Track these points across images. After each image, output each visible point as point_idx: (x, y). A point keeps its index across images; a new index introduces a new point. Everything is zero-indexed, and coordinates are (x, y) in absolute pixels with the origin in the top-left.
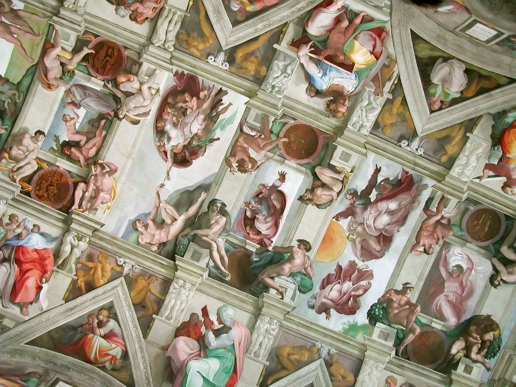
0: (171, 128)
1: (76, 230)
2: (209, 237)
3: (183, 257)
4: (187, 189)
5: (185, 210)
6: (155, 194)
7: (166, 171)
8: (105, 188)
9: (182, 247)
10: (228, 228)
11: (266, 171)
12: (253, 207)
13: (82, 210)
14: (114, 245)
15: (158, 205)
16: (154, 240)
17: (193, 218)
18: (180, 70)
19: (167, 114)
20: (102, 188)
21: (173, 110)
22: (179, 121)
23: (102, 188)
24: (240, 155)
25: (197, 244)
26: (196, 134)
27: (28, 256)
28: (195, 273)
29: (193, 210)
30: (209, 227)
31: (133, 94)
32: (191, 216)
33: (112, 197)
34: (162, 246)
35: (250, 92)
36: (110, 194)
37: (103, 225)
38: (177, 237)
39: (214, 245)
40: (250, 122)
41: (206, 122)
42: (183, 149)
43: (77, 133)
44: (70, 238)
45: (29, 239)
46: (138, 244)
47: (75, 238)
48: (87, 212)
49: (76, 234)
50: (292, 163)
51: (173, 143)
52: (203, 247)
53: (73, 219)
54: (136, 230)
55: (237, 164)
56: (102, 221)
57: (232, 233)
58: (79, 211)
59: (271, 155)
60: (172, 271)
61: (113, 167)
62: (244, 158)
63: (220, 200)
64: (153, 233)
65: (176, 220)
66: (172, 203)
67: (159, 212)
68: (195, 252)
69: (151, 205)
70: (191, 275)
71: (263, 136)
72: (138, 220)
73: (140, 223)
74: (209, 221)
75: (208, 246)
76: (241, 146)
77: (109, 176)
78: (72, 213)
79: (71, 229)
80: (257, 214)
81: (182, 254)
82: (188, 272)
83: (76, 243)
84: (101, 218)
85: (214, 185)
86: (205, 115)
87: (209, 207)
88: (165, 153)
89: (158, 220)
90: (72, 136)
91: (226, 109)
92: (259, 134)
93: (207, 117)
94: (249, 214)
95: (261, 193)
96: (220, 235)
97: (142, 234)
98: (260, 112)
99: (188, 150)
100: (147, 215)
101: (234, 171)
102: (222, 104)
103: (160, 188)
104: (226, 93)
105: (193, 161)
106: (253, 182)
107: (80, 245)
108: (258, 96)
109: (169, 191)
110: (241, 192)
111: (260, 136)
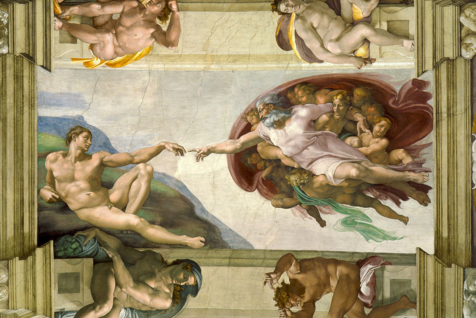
0: (302, 118)
1: (12, 18)
2: (119, 289)
3: (56, 257)
4: (193, 202)
5: (151, 219)
6: (155, 143)
7: (212, 144)
8: (124, 38)
9: (74, 246)
13: (60, 12)
14: (19, 110)
15: (137, 159)
16: (63, 185)
17: (143, 242)
18: (431, 89)
19: (328, 98)
20: (121, 32)
21: (341, 108)
22: (323, 128)
23: (121, 32)
25: (95, 272)
26: (312, 175)
28: (34, 296)
31: (338, 12)
32: (144, 234)
33: (113, 61)
34: (57, 206)
35: (449, 251)
36: (117, 54)
37: (47, 67)
39: (107, 308)
40: (386, 274)
41: (346, 184)
42: (270, 161)
46: (43, 157)
48: (59, 24)
49: (5, 22)
54: (69, 140)
55: (287, 282)
56: (55, 63)
58: (55, 7)
60: (18, 249)
61: (173, 36)
62: (307, 291)
63: (201, 279)
64: (77, 175)
65: (124, 209)
67: (123, 168)
68: (76, 277)
69: (131, 145)
70: (26, 289)
71: (367, 311)
72: (90, 132)
73: (85, 142)
74: (152, 275)
76: (328, 276)
77: (153, 36)
79: (10, 7)
81: (60, 254)
82: (30, 284)
84: (60, 58)
85: (227, 253)
86: (358, 176)
87: (177, 263)
88: (248, 128)
91: (392, 215)
92: (369, 302)
93: (354, 184)
96: (132, 309)
98: (415, 285)
99: (272, 171)
101: (272, 280)
102: (398, 204)
103: (174, 149)
104: (425, 202)
105: (256, 191)
108: (447, 270)
109: (175, 168)
111: (366, 305)
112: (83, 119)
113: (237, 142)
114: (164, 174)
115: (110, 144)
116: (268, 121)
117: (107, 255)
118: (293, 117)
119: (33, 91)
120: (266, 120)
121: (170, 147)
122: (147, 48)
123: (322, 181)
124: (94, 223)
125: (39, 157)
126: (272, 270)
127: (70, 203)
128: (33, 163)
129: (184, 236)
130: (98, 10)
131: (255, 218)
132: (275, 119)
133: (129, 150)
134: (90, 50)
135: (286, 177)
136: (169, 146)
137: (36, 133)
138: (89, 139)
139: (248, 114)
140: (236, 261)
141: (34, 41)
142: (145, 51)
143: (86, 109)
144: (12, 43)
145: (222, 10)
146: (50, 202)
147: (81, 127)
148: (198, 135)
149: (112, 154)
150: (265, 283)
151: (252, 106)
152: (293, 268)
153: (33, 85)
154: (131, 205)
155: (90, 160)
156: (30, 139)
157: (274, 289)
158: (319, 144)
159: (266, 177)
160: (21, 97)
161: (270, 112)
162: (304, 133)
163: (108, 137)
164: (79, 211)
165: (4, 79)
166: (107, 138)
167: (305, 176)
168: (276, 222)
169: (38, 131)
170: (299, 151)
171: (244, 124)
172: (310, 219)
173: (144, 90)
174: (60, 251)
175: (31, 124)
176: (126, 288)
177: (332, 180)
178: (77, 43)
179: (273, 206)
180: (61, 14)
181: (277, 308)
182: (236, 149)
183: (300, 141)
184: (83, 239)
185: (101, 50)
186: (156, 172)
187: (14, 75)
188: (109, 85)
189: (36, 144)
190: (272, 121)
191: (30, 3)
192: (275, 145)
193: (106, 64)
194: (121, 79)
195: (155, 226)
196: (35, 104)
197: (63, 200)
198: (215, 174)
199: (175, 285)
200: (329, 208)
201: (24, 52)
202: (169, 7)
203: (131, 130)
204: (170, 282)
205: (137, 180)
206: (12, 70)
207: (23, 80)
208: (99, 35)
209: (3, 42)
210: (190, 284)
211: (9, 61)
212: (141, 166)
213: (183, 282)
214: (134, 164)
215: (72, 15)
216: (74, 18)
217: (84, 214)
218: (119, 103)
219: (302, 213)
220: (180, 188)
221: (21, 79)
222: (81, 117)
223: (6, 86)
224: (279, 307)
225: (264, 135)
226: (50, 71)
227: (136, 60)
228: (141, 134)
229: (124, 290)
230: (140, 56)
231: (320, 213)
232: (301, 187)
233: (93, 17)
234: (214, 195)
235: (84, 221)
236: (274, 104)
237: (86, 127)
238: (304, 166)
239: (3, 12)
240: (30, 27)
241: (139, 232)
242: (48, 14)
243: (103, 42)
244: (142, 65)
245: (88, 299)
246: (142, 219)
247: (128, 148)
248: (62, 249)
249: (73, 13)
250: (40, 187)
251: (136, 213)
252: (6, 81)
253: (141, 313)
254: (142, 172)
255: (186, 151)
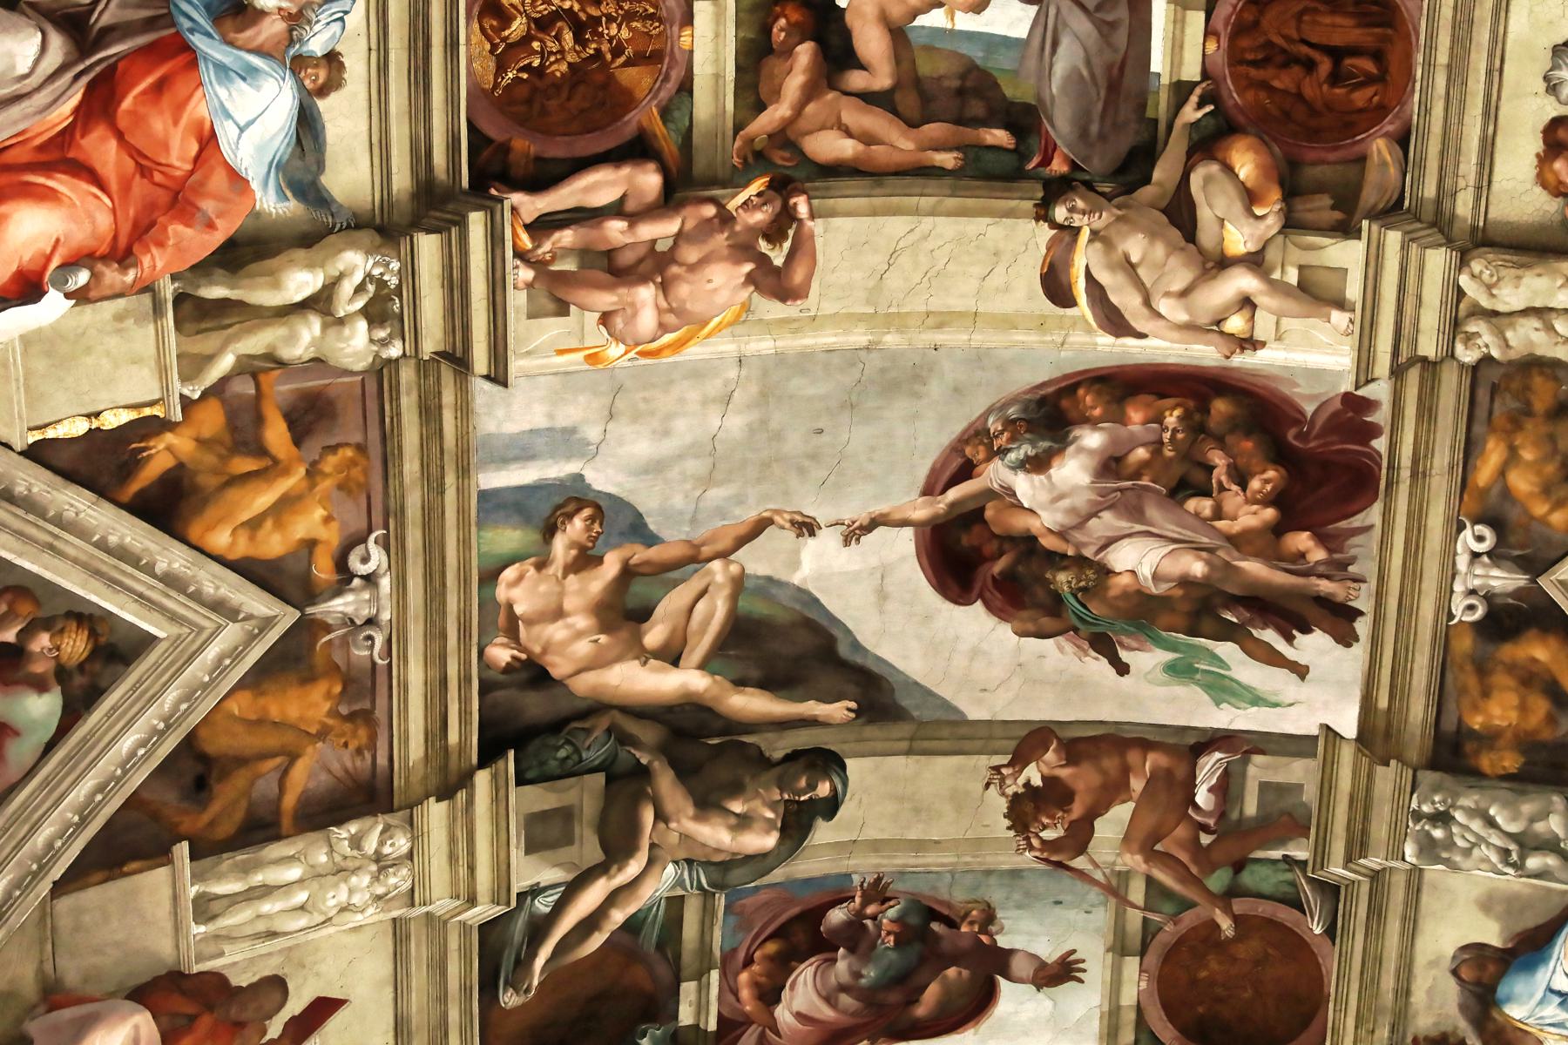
1: (410, 271)
2: (662, 826)
4: (835, 632)
6: (749, 514)
8: (683, 290)
9: (562, 753)
10: (736, 875)
11: (1058, 903)
12: (874, 918)
13: (529, 245)
15: (706, 551)
16: (536, 629)
20: (677, 277)
23: (677, 277)
24: (1082, 779)
26: (1106, 572)
27: (158, 124)
29: (751, 703)
30: (707, 804)
34: (524, 675)
36: (663, 328)
37: (498, 377)
38: (597, 708)
39: (634, 868)
43: (898, 34)
44: (355, 263)
45: (249, 74)
46: (490, 577)
47: (371, 288)
48: (526, 274)
49: (394, 281)
50: (1134, 983)
51: (1025, 486)
52: (602, 828)
53: (462, 224)
54: (550, 531)
55: (1037, 781)
56: (515, 366)
57: (721, 901)
58: (515, 234)
59: (1137, 893)
62: (1077, 798)
63: (845, 783)
64: (568, 604)
65: (675, 662)
66: (744, 604)
68: (566, 816)
69: (694, 521)
71: (1206, 839)
72: (598, 507)
73: (588, 529)
74: (736, 789)
75: (617, 846)
78: (491, 207)
80: (852, 950)
81: (530, 775)
83: (347, 303)
84: (529, 353)
85: (903, 729)
88: (966, 471)
89: (639, 588)
90: (870, 9)
94: (837, 916)
95: (952, 924)
96: (689, 862)
97: (541, 566)
99: (1017, 562)
100: (638, 530)
101: (1003, 779)
103: (793, 522)
105: (979, 603)
106: (988, 873)
107: (347, 331)
109: (795, 564)
110: (919, 846)
111: (1205, 828)
112: (584, 480)
113: (939, 502)
114: (769, 579)
115: (645, 525)
116: (1012, 456)
117: (638, 761)
118: (1071, 449)
119: (465, 438)
120: (1009, 455)
121: (785, 520)
122: (736, 308)
123: (1126, 586)
124: (606, 699)
125: (481, 581)
126: (1004, 759)
127: (553, 665)
128: (468, 596)
129: (812, 702)
130: (621, 233)
131: (972, 659)
132: (1029, 453)
133: (688, 533)
134: (601, 326)
135: (1048, 575)
136: (783, 518)
137: (474, 529)
138: (598, 521)
139: (967, 442)
140: (926, 744)
141: (465, 319)
142: (729, 315)
143: (589, 457)
144: (412, 330)
145: (916, 212)
146: (508, 669)
147: (577, 499)
148: (850, 489)
149: (650, 546)
150: (987, 785)
151: (979, 425)
152: (1050, 756)
153: (465, 424)
154: (692, 650)
155: (599, 568)
156: (461, 543)
157: (1007, 797)
158: (1126, 507)
159: (1001, 573)
160: (438, 455)
161: (1018, 436)
162: (1093, 482)
163: (641, 510)
164: (573, 678)
165: (395, 419)
166: (638, 511)
167: (1090, 573)
168: (1020, 665)
169: (480, 525)
170: (1079, 520)
171: (957, 462)
172: (1096, 659)
173: (728, 399)
174: (530, 768)
175: (462, 511)
176: (678, 822)
177: (1150, 583)
178: (568, 315)
179: (1015, 633)
180: (529, 251)
181: (1012, 833)
182: (935, 517)
183: (1081, 501)
184: (582, 736)
185: (626, 324)
186: (749, 576)
187: (420, 407)
188: (645, 400)
189: (474, 553)
190: (1022, 457)
191: (453, 230)
192: (1026, 505)
193: (637, 353)
194: (671, 382)
195: (747, 689)
196: (471, 466)
197: (537, 660)
198: (884, 572)
199: (787, 801)
200: (1137, 640)
201: (441, 348)
202: (792, 212)
203: (694, 489)
204: (776, 795)
205: (706, 596)
206: (414, 396)
207: (440, 415)
208: (623, 291)
209: (388, 330)
210: (821, 796)
211: (407, 374)
212: (716, 565)
213: (805, 795)
214: (699, 562)
215: (557, 251)
216: (563, 257)
217: (584, 684)
218: (666, 433)
219: (1078, 647)
220: (805, 604)
221: (437, 413)
222: (579, 478)
223: (399, 435)
224: (1016, 831)
225: (1001, 486)
226: (505, 384)
227: (708, 336)
228: (717, 494)
229: (673, 825)
230: (719, 328)
231: (1118, 648)
232: (1079, 595)
233: (610, 251)
234: (881, 612)
235: (584, 699)
236: (1028, 421)
237: (591, 496)
238: (1088, 552)
239: (387, 259)
240: (455, 288)
241: (710, 704)
242: (498, 252)
243: (633, 305)
244: (725, 346)
245: (590, 850)
246: (718, 677)
247: (687, 529)
248: (535, 763)
249: (559, 245)
250: (483, 643)
251: (703, 666)
252: (399, 421)
253: (712, 868)
254: (719, 578)
255: (822, 526)
